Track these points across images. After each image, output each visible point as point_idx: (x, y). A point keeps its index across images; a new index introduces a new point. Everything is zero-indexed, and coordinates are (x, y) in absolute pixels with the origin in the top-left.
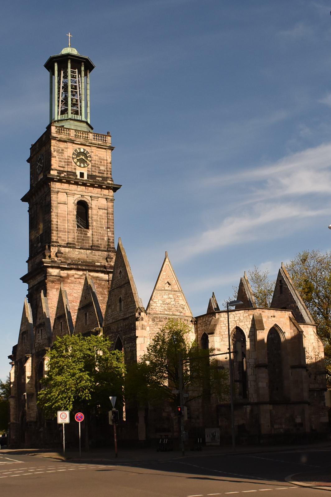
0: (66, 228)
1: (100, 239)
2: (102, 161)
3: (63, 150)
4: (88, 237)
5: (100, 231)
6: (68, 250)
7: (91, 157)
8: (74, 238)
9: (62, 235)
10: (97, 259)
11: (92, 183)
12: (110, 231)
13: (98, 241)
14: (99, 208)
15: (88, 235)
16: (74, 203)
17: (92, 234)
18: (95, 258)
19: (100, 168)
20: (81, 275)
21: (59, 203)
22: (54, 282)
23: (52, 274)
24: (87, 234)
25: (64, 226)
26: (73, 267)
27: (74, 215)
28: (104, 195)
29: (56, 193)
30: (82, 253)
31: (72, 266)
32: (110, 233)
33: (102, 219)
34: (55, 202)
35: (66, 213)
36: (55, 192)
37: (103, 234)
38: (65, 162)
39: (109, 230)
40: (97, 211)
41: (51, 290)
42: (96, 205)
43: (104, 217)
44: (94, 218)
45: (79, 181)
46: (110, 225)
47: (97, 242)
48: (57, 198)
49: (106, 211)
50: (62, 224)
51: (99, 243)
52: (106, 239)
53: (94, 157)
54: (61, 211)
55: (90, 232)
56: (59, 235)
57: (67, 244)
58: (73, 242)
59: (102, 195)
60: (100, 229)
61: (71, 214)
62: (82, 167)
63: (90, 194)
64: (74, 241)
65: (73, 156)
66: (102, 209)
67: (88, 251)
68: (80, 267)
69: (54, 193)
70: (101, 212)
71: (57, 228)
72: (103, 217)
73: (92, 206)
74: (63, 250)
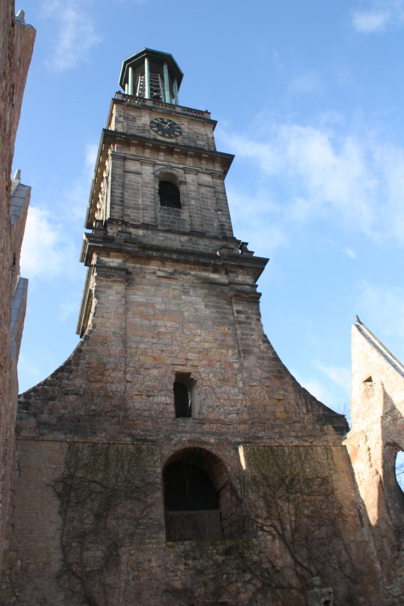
0: (139, 205)
1: (206, 224)
2: (200, 136)
3: (134, 119)
4: (184, 220)
5: (205, 214)
6: (143, 232)
7: (179, 128)
8: (155, 218)
9: (132, 212)
10: (202, 250)
11: (183, 148)
12: (223, 214)
13: (202, 225)
14: (199, 185)
15: (181, 217)
16: (154, 173)
17: (190, 216)
18: (197, 248)
19: (196, 142)
20: (171, 274)
21: (125, 172)
22: (110, 278)
23: (107, 265)
24: (179, 216)
25: (135, 201)
26: (153, 254)
27: (154, 188)
28: (206, 169)
29: (121, 158)
30: (170, 239)
31: (149, 252)
32: (224, 217)
33: (207, 198)
34: (118, 170)
35: (140, 185)
36: (119, 157)
37: (210, 218)
38: (136, 130)
39: (219, 213)
40: (196, 187)
41: (104, 292)
42: (193, 180)
43: (209, 196)
44: (190, 194)
45: (159, 143)
46: (220, 206)
47: (200, 227)
48: (124, 166)
49: (212, 190)
50: (131, 198)
51: (204, 229)
52: (218, 225)
53: (186, 130)
54: (130, 181)
55: (185, 214)
56: (125, 213)
57: (143, 224)
58: (153, 224)
59: (202, 169)
60: (205, 211)
61: (148, 186)
62: (167, 137)
63: (182, 166)
64: (155, 222)
65: (152, 125)
66: (206, 186)
67: (182, 238)
68: (165, 255)
69: (118, 158)
70: (204, 190)
71: (122, 201)
72: (207, 196)
73: (187, 181)
74: (132, 230)
